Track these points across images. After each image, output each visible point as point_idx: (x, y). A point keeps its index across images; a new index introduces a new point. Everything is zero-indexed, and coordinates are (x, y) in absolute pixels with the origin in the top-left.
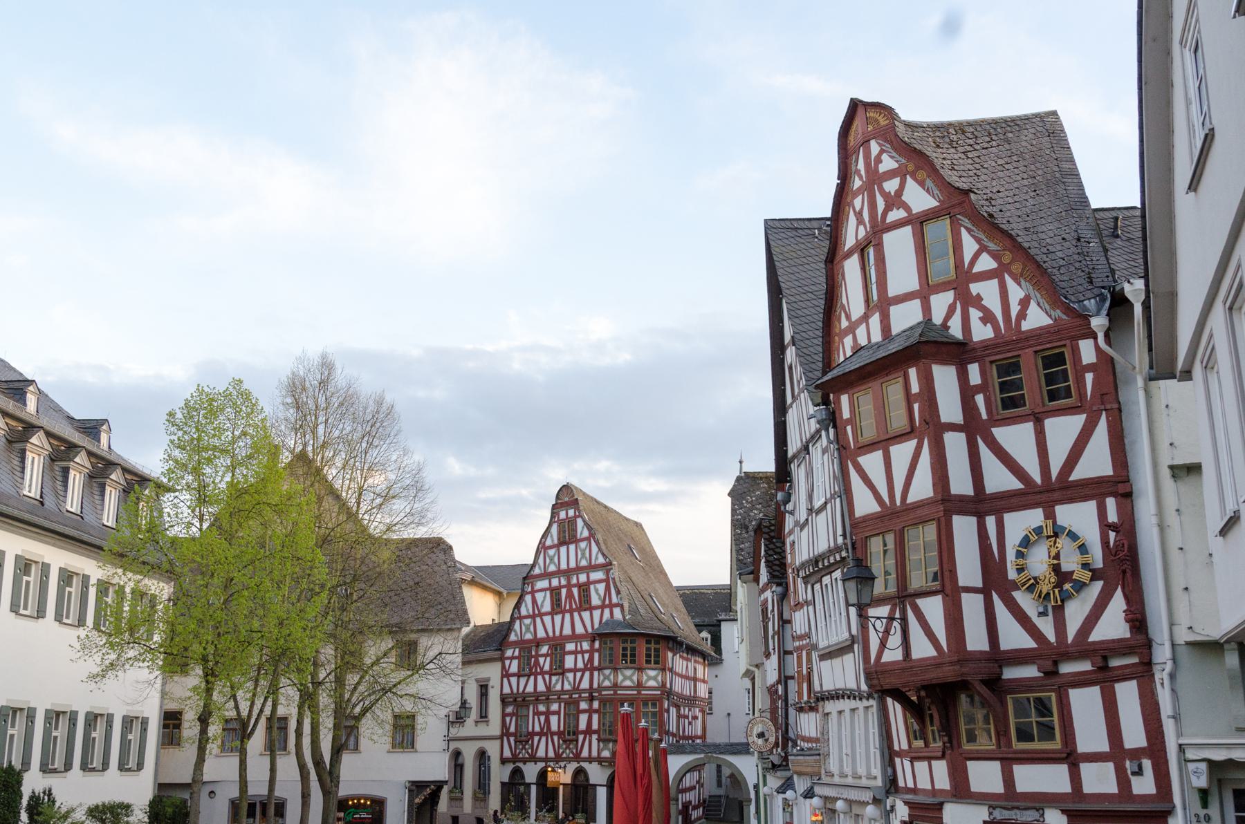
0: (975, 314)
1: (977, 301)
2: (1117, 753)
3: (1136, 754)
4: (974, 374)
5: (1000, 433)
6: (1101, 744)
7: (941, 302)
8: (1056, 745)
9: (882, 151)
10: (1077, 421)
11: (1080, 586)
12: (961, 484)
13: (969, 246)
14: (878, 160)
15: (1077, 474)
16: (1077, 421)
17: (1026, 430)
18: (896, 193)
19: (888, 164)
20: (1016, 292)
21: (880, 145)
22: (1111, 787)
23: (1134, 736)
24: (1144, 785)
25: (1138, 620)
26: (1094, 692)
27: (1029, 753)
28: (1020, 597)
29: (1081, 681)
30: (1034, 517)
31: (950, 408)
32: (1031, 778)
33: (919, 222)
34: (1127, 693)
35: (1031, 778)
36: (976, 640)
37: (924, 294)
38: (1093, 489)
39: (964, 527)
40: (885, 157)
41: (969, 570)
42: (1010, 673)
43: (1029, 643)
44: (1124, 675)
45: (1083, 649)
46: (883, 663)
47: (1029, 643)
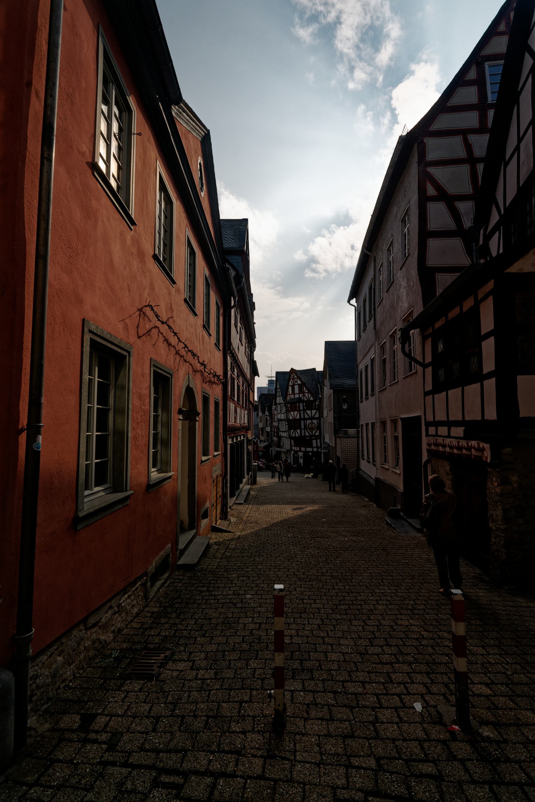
0: (305, 397)
1: (305, 396)
2: (317, 447)
3: (319, 447)
4: (304, 404)
5: (307, 411)
7: (301, 395)
10: (315, 411)
11: (314, 429)
12: (302, 417)
13: (305, 389)
15: (315, 417)
16: (315, 411)
17: (310, 411)
19: (295, 377)
20: (310, 395)
22: (316, 450)
23: (319, 445)
24: (319, 450)
25: (320, 433)
30: (310, 421)
31: (301, 408)
32: (308, 449)
33: (298, 385)
34: (319, 441)
35: (308, 449)
36: (303, 435)
37: (299, 394)
38: (316, 419)
39: (302, 422)
41: (303, 427)
42: (307, 438)
43: (308, 435)
44: (318, 439)
47: (308, 435)
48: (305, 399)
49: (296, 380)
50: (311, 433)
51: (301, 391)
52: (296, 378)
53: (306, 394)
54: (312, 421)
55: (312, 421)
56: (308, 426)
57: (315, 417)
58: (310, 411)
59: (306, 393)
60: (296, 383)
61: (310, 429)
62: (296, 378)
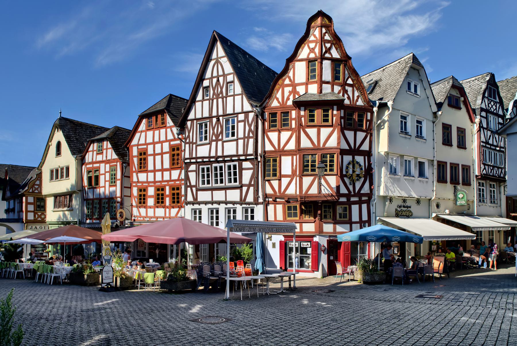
6: (357, 219)
8: (347, 219)
9: (326, 33)
14: (324, 35)
17: (353, 133)
18: (329, 48)
19: (327, 37)
21: (326, 30)
26: (357, 206)
27: (464, 221)
28: (345, 179)
29: (355, 203)
33: (333, 60)
40: (327, 34)
45: (359, 194)
46: (286, 194)
48: (347, 102)
49: (328, 45)
50: (351, 188)
51: (337, 78)
52: (328, 41)
53: (349, 89)
54: (353, 158)
55: (353, 158)
56: (347, 168)
57: (362, 148)
58: (353, 133)
59: (350, 85)
60: (327, 55)
61: (350, 177)
62: (328, 41)
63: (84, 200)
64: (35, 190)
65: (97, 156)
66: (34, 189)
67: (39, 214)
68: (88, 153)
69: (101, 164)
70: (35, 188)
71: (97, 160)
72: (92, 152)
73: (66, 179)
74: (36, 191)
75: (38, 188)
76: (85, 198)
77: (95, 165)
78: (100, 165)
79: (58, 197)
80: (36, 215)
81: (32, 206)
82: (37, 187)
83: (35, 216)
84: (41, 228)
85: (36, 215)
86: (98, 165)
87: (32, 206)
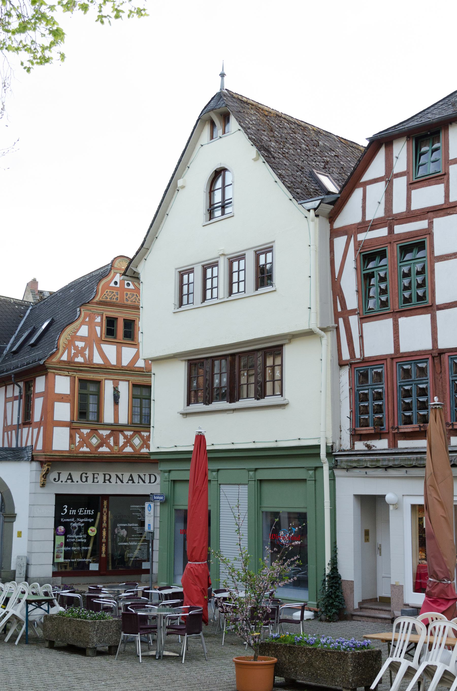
63: (342, 364)
64: (76, 355)
65: (414, 192)
66: (73, 351)
67: (85, 431)
68: (358, 193)
69: (436, 221)
70: (76, 348)
71: (415, 206)
72: (382, 186)
73: (257, 292)
74: (80, 359)
75: (84, 349)
76: (346, 356)
77: (399, 229)
78: (431, 224)
79: (217, 363)
80: (77, 436)
81: (67, 406)
82: (80, 344)
83: (72, 438)
84: (84, 479)
85: (77, 436)
86: (422, 225)
87: (67, 406)
